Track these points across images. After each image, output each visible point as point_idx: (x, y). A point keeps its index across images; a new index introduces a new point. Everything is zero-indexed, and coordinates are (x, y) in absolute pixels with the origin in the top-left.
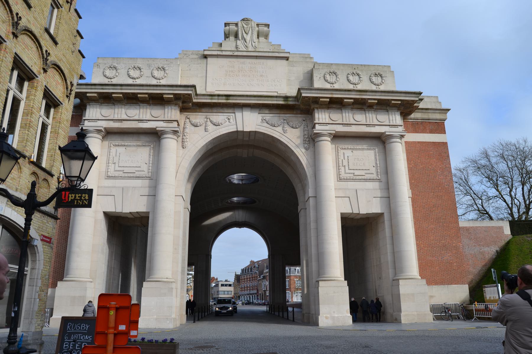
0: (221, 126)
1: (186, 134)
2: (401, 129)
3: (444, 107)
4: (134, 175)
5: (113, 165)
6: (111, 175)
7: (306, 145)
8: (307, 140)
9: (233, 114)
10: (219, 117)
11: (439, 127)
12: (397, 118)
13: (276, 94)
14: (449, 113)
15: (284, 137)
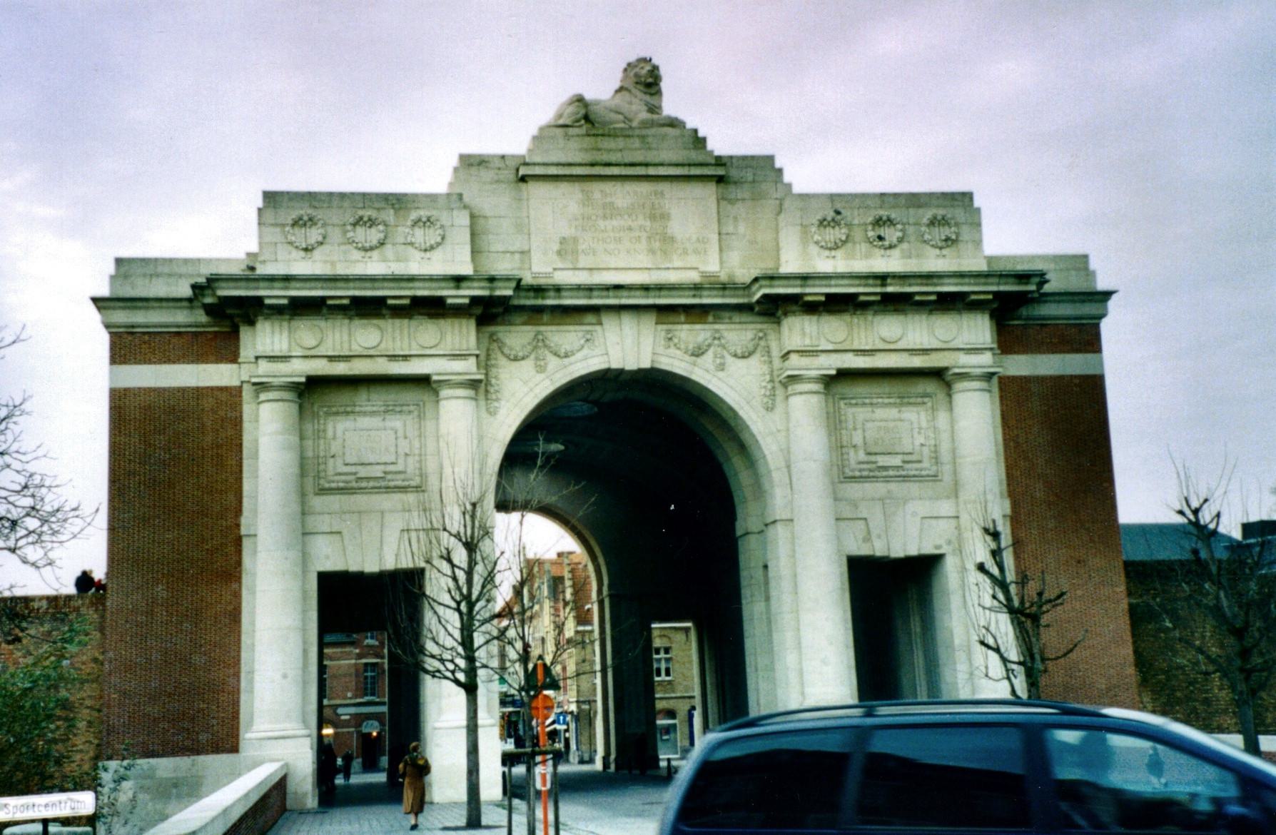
0: (572, 359)
1: (493, 381)
2: (986, 359)
3: (1101, 285)
4: (383, 484)
5: (331, 461)
6: (327, 485)
7: (765, 400)
8: (769, 386)
9: (598, 328)
10: (566, 336)
11: (1085, 337)
12: (976, 330)
13: (694, 277)
14: (1112, 303)
15: (714, 380)
